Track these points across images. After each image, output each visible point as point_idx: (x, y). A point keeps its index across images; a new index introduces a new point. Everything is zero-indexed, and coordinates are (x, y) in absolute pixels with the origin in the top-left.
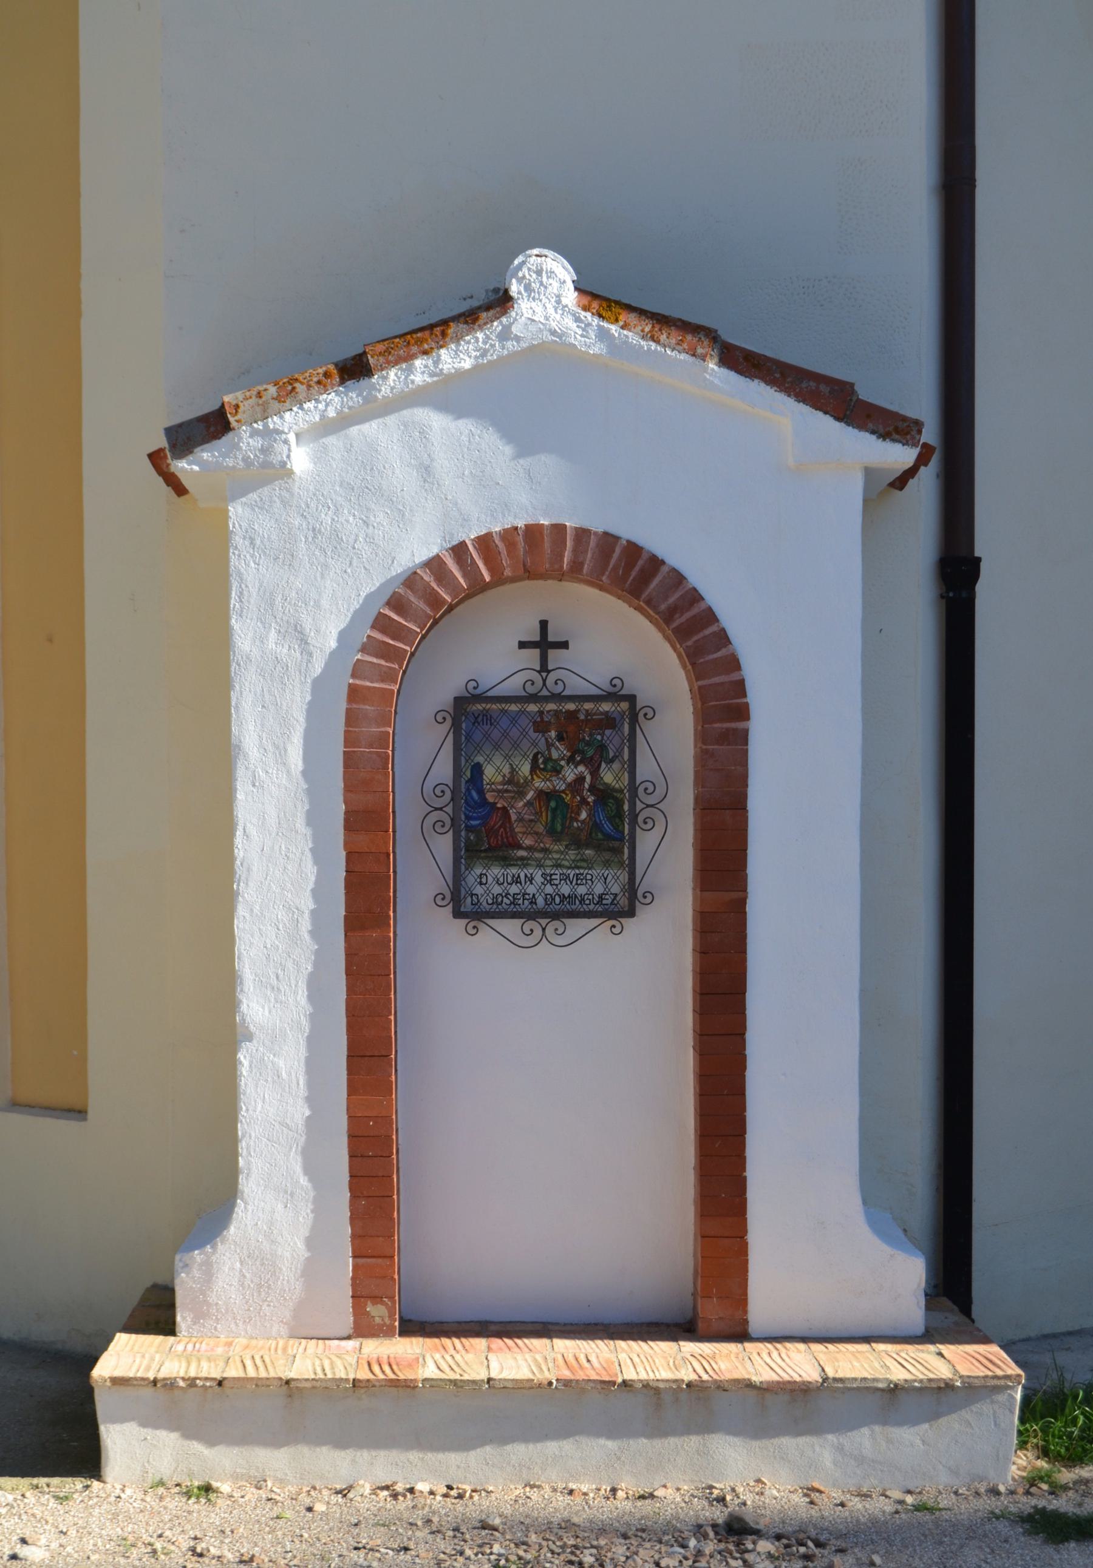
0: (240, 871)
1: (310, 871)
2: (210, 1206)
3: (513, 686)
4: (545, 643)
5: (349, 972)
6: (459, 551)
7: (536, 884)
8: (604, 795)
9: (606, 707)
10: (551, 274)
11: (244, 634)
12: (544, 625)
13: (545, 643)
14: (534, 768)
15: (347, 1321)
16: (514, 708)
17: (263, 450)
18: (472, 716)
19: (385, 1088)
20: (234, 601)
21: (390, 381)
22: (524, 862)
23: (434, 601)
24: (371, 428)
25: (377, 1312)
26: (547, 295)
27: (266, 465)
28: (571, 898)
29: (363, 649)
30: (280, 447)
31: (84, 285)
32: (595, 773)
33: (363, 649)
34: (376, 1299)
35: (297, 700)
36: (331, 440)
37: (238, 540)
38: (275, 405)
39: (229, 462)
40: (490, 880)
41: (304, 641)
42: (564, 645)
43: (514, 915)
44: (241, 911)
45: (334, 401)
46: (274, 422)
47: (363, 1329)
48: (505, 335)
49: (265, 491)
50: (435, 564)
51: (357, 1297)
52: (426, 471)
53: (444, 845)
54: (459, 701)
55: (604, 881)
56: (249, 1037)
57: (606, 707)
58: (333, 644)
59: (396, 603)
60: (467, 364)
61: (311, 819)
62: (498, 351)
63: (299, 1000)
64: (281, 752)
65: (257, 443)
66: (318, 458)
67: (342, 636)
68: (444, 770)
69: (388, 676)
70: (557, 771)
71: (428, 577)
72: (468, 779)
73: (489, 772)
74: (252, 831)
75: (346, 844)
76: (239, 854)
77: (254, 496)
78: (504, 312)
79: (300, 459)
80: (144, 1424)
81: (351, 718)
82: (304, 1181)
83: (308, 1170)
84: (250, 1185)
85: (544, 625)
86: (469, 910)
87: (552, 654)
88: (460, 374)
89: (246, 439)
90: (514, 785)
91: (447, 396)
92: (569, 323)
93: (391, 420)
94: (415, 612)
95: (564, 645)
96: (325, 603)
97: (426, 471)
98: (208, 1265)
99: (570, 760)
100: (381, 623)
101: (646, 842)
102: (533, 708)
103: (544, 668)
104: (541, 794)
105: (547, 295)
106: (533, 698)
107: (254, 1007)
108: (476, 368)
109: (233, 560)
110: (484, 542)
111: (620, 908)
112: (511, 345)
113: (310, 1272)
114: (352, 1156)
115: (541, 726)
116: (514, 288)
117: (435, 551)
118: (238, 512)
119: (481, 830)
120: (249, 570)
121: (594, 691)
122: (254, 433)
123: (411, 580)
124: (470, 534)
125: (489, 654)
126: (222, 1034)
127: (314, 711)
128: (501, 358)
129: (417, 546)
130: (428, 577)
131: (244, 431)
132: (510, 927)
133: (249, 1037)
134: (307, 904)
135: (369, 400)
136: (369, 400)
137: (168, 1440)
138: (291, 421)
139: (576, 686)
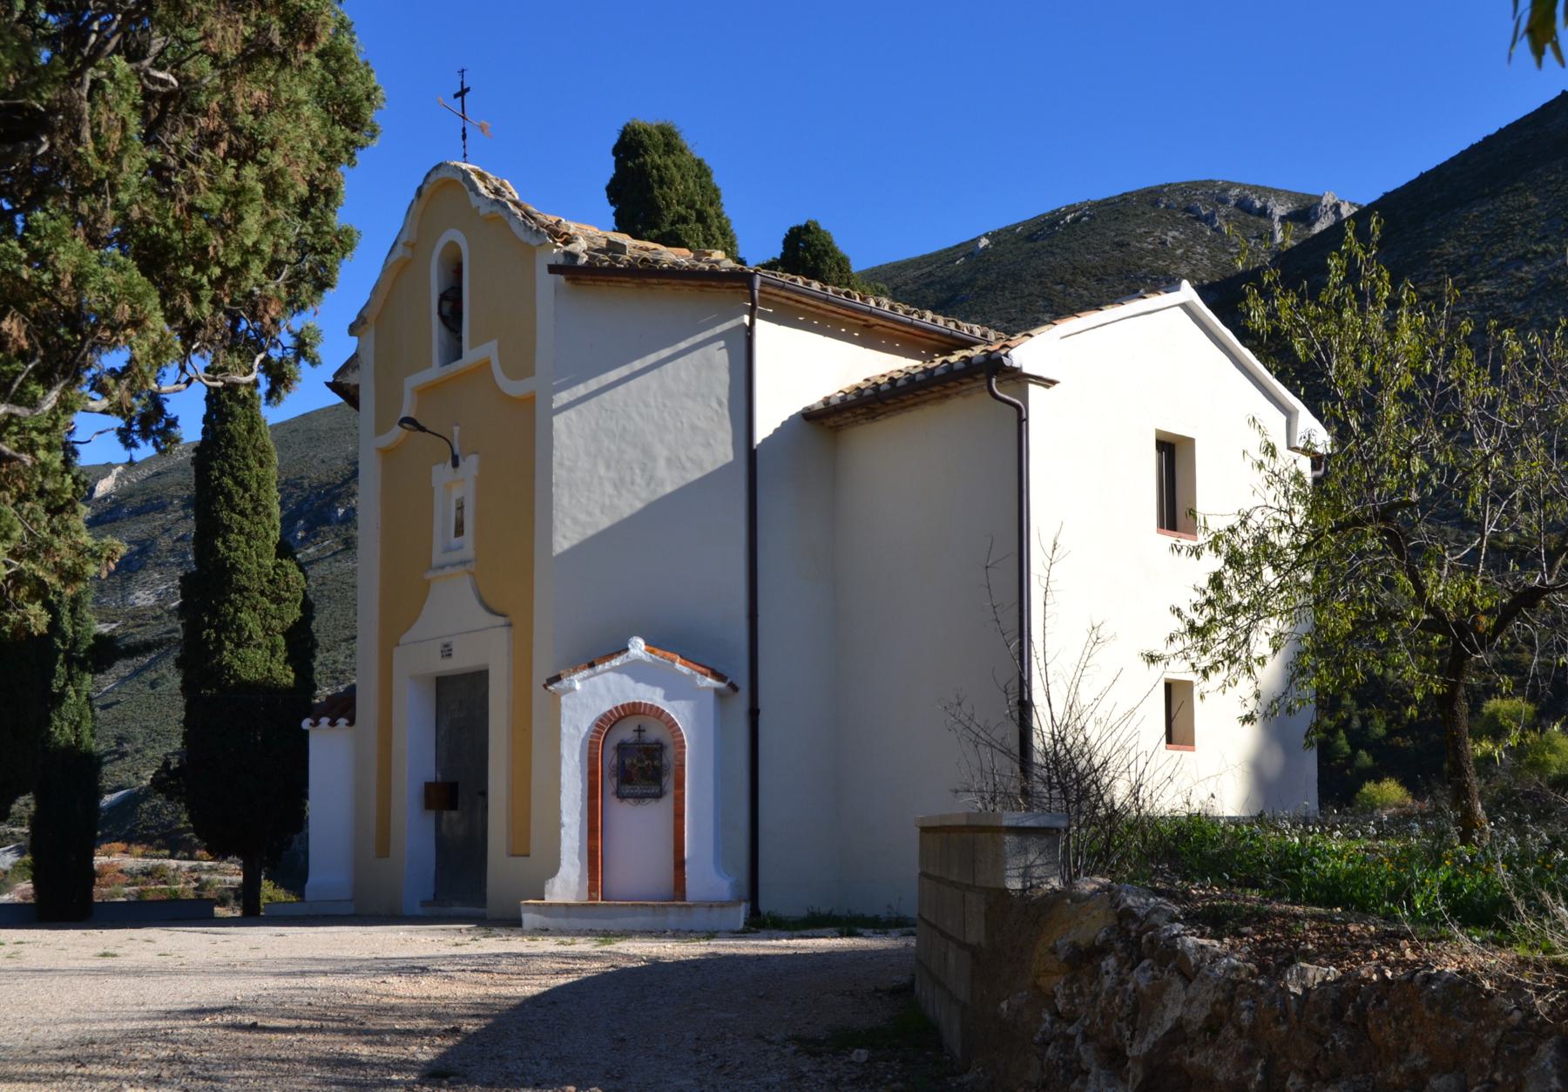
1: (580, 785)
2: (553, 869)
7: (638, 790)
8: (655, 768)
11: (565, 728)
13: (640, 730)
18: (622, 748)
21: (600, 668)
26: (638, 647)
35: (577, 744)
40: (627, 789)
45: (586, 673)
52: (609, 689)
53: (615, 780)
55: (654, 790)
63: (577, 817)
68: (615, 761)
72: (621, 765)
73: (628, 762)
84: (564, 863)
86: (621, 796)
90: (633, 765)
97: (609, 689)
101: (665, 779)
105: (638, 647)
107: (565, 819)
111: (658, 796)
124: (619, 704)
125: (626, 733)
126: (558, 825)
129: (606, 707)
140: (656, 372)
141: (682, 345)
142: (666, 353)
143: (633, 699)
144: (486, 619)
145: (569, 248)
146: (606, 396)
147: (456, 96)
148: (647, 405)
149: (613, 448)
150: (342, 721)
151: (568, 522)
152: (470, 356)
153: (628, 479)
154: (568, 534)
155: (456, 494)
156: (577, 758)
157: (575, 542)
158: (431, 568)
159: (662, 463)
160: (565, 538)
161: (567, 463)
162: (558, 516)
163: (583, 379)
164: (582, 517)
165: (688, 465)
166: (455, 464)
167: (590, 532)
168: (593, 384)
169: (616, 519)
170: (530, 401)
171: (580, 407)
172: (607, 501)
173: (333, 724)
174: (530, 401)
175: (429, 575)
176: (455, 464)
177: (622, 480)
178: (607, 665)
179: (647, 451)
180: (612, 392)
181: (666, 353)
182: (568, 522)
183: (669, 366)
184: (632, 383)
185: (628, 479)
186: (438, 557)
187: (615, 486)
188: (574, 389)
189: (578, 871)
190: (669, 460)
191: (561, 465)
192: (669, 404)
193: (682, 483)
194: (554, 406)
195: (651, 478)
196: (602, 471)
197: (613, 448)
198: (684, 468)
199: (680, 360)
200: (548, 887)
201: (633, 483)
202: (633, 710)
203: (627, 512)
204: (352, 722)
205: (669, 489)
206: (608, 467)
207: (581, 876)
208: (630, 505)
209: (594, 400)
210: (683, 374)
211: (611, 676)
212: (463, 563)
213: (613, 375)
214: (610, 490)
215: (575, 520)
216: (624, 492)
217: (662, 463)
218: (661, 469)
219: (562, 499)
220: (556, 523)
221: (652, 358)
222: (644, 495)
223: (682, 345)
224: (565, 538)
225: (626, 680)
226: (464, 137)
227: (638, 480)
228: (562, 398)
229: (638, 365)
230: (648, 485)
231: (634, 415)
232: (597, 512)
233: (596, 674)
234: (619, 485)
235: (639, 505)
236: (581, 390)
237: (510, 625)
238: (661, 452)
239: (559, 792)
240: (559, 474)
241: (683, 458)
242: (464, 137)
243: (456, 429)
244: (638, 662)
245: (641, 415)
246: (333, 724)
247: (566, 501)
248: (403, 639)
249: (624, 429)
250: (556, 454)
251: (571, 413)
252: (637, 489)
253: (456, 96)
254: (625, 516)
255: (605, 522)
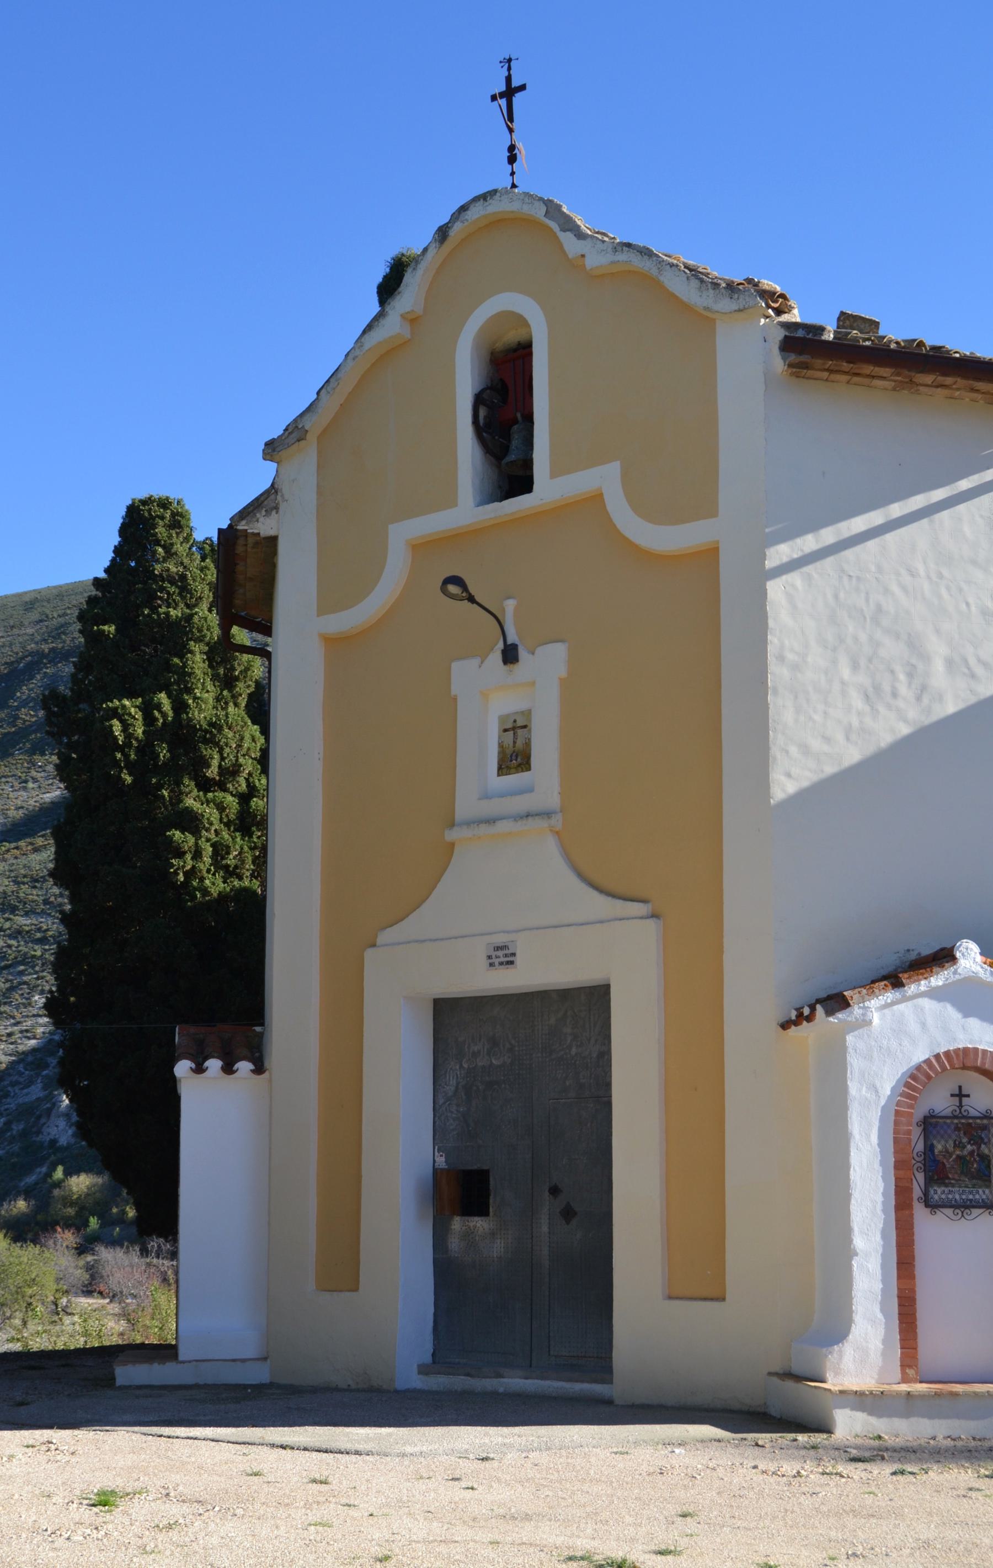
0: (852, 1185)
1: (881, 1185)
3: (948, 1112)
4: (960, 1095)
5: (897, 1228)
6: (937, 1056)
7: (957, 1195)
9: (985, 1121)
10: (971, 950)
11: (854, 1088)
12: (960, 1087)
13: (960, 1095)
14: (955, 1146)
15: (898, 1376)
16: (948, 1121)
17: (864, 1015)
18: (930, 1123)
19: (912, 1277)
20: (849, 1075)
21: (911, 989)
22: (953, 1186)
23: (929, 1078)
24: (901, 1007)
25: (911, 1372)
26: (970, 957)
27: (863, 1020)
28: (971, 1200)
29: (901, 1095)
30: (869, 1014)
31: (725, 940)
32: (979, 1148)
33: (901, 1095)
34: (910, 1367)
35: (875, 1116)
36: (886, 1011)
37: (850, 1050)
38: (867, 997)
39: (849, 1019)
40: (939, 1193)
41: (877, 1091)
42: (968, 1096)
43: (951, 1207)
44: (853, 1202)
45: (890, 996)
46: (867, 1004)
47: (905, 1380)
48: (955, 973)
49: (861, 1031)
50: (927, 1061)
51: (903, 1366)
52: (923, 1025)
53: (920, 1177)
54: (925, 1117)
56: (856, 1254)
57: (985, 1121)
58: (888, 1093)
59: (913, 1077)
60: (940, 983)
61: (882, 1163)
62: (953, 978)
63: (877, 1238)
64: (868, 1137)
65: (861, 1011)
66: (882, 1018)
67: (893, 1089)
68: (920, 1147)
69: (911, 1107)
70: (964, 1147)
71: (925, 1067)
72: (929, 1148)
73: (939, 1147)
74: (857, 1168)
75: (895, 1174)
76: (852, 1177)
77: (856, 1033)
78: (955, 964)
79: (876, 1019)
80: (852, 1409)
81: (896, 1123)
82: (880, 1316)
83: (882, 1311)
85: (960, 1087)
87: (964, 1099)
88: (938, 988)
89: (856, 1010)
90: (947, 1153)
91: (934, 994)
92: (979, 968)
93: (910, 1004)
94: (918, 1079)
95: (968, 1096)
96: (885, 1076)
97: (923, 1025)
98: (840, 1351)
99: (969, 1143)
100: (907, 1085)
102: (956, 1121)
103: (961, 1106)
104: (958, 1156)
106: (955, 1117)
107: (859, 1242)
108: (944, 985)
109: (848, 1058)
110: (947, 1054)
112: (957, 977)
113: (884, 1354)
114: (900, 1305)
115: (957, 1128)
116: (958, 955)
117: (927, 1057)
118: (850, 1039)
119: (935, 1171)
120: (855, 1062)
121: (978, 1114)
122: (860, 1008)
123: (919, 1068)
125: (939, 1101)
127: (882, 1120)
128: (954, 982)
129: (920, 1055)
130: (925, 1067)
131: (856, 1007)
132: (949, 1211)
133: (856, 1254)
134: (880, 1198)
135: (904, 996)
136: (904, 996)
137: (860, 1416)
138: (874, 1003)
139: (973, 1113)
140: (925, 521)
141: (964, 484)
142: (939, 495)
143: (962, 1042)
144: (601, 905)
145: (785, 318)
146: (849, 554)
147: (522, 88)
148: (913, 573)
149: (863, 637)
150: (244, 1067)
151: (793, 750)
152: (548, 486)
153: (887, 688)
154: (795, 771)
155: (504, 703)
156: (874, 1138)
157: (805, 784)
158: (452, 825)
159: (939, 666)
160: (787, 780)
161: (790, 656)
162: (777, 741)
163: (814, 526)
164: (816, 744)
165: (979, 671)
166: (510, 655)
167: (830, 769)
168: (828, 536)
169: (870, 750)
170: (710, 555)
171: (809, 569)
172: (855, 722)
173: (228, 1069)
174: (710, 555)
175: (451, 835)
176: (510, 655)
177: (877, 688)
178: (923, 985)
179: (914, 645)
180: (858, 549)
181: (939, 495)
182: (793, 750)
183: (945, 515)
184: (889, 537)
185: (887, 688)
186: (467, 803)
187: (867, 697)
188: (799, 541)
189: (881, 1331)
190: (949, 663)
191: (781, 658)
192: (945, 572)
193: (973, 700)
194: (769, 564)
195: (924, 688)
196: (846, 672)
197: (863, 637)
198: (973, 676)
199: (962, 508)
200: (832, 1359)
201: (895, 695)
202: (964, 1060)
203: (886, 739)
204: (259, 1069)
205: (951, 707)
206: (855, 666)
207: (885, 1341)
208: (890, 728)
209: (830, 560)
210: (967, 529)
211: (926, 1003)
212: (547, 814)
213: (859, 524)
214: (858, 702)
215: (805, 750)
216: (881, 709)
217: (939, 666)
218: (938, 675)
219: (782, 710)
220: (775, 751)
221: (918, 502)
222: (912, 714)
223: (964, 484)
224: (787, 780)
225: (951, 1012)
226: (512, 159)
227: (903, 690)
228: (780, 553)
229: (896, 510)
230: (919, 699)
231: (895, 588)
232: (840, 737)
233: (905, 999)
234: (872, 695)
235: (905, 730)
236: (809, 543)
237: (654, 916)
238: (938, 649)
239: (848, 1197)
240: (777, 673)
241: (972, 661)
242: (512, 159)
243: (510, 605)
244: (972, 981)
245: (904, 589)
246: (228, 1069)
247: (788, 716)
248: (383, 938)
249: (879, 608)
250: (773, 641)
251: (795, 578)
252: (901, 704)
253: (522, 88)
254: (883, 744)
255: (853, 755)
